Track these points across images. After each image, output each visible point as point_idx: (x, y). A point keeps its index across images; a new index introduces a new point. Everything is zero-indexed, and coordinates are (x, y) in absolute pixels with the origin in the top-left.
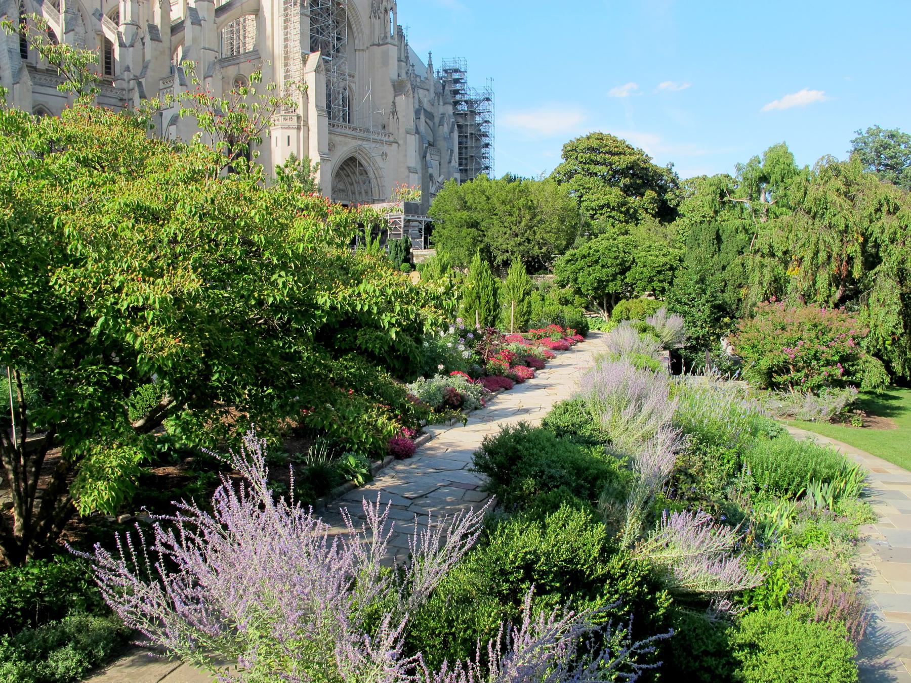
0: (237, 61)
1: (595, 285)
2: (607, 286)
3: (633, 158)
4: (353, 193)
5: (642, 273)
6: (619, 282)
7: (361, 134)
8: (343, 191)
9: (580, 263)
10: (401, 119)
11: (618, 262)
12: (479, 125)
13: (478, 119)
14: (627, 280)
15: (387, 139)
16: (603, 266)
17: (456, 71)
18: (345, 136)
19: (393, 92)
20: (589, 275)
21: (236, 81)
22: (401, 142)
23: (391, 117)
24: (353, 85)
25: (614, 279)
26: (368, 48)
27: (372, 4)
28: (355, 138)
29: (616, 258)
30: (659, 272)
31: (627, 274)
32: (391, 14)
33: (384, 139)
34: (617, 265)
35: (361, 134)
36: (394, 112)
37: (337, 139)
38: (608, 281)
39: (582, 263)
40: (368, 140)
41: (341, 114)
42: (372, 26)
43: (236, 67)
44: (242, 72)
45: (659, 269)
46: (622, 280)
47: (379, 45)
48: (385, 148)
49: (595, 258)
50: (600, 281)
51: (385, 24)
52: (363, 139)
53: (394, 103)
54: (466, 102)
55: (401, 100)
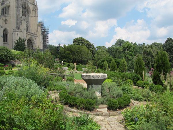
3: (88, 42)
4: (30, 47)
7: (32, 35)
12: (46, 34)
13: (46, 33)
17: (42, 23)
28: (30, 35)
37: (27, 35)
40: (33, 36)
44: (6, 19)
47: (34, 16)
48: (35, 37)
52: (32, 35)
54: (44, 29)
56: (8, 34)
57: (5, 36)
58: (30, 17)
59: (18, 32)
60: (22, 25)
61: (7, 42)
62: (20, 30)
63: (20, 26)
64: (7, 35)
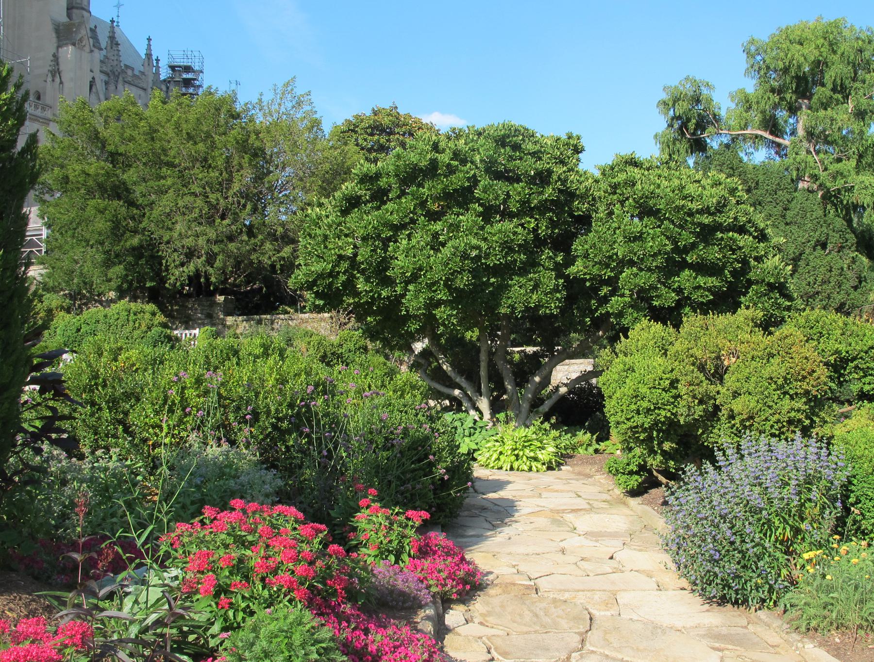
1: (463, 281)
2: (503, 288)
5: (639, 238)
6: (549, 280)
9: (393, 211)
10: (67, 85)
11: (549, 192)
14: (577, 268)
16: (488, 214)
19: (55, 40)
20: (436, 244)
23: (49, 79)
25: (532, 264)
29: (543, 178)
30: (706, 234)
31: (577, 247)
34: (543, 208)
36: (56, 72)
38: (504, 271)
39: (407, 203)
45: (706, 220)
46: (559, 270)
49: (457, 181)
50: (479, 270)
53: (56, 58)
55: (68, 52)
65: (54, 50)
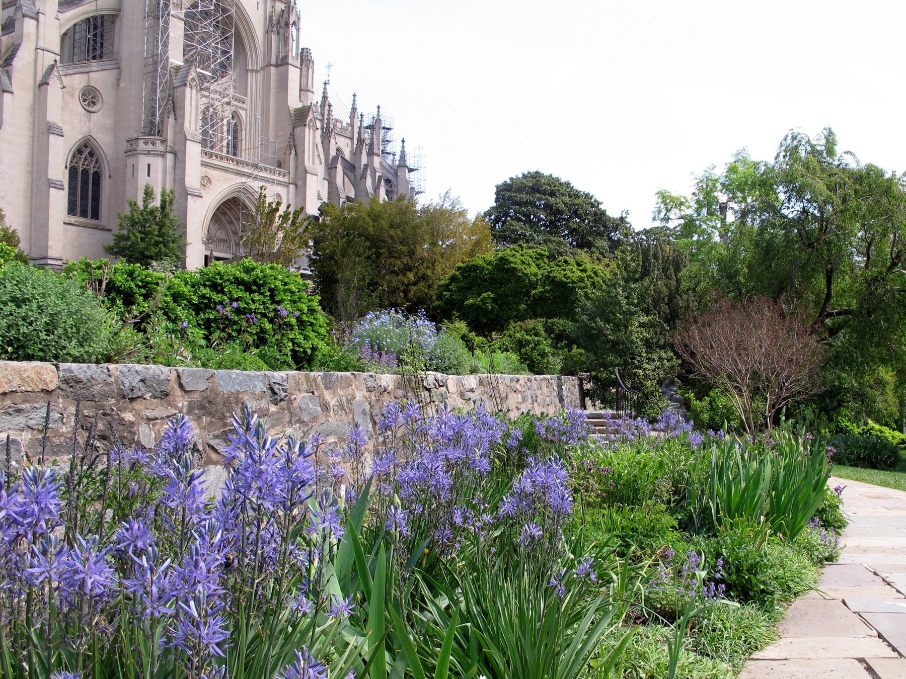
0: (87, 70)
7: (246, 170)
8: (225, 241)
15: (281, 179)
18: (226, 170)
19: (291, 122)
21: (84, 94)
22: (300, 183)
23: (288, 152)
24: (243, 113)
26: (262, 69)
27: (271, 17)
28: (239, 173)
32: (293, 30)
33: (276, 177)
35: (246, 170)
37: (213, 174)
40: (256, 178)
41: (225, 143)
42: (268, 43)
43: (85, 76)
44: (92, 84)
51: (286, 41)
52: (249, 176)
53: (292, 135)
56: (105, 174)
57: (85, 183)
58: (252, 71)
59: (148, 153)
60: (178, 112)
61: (96, 215)
62: (164, 142)
63: (166, 119)
64: (97, 177)
65: (289, 130)
